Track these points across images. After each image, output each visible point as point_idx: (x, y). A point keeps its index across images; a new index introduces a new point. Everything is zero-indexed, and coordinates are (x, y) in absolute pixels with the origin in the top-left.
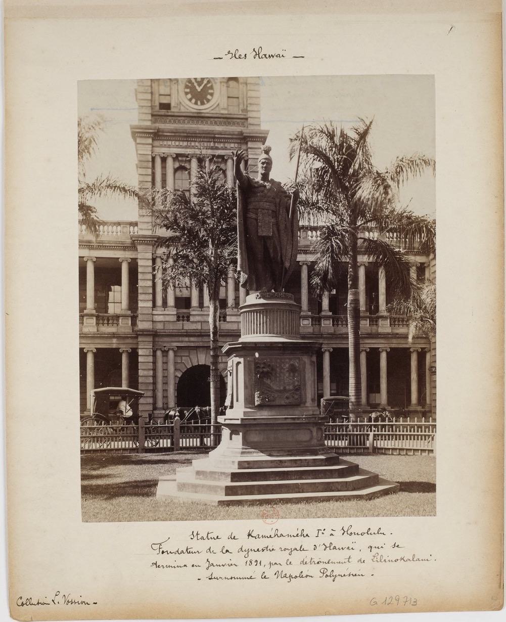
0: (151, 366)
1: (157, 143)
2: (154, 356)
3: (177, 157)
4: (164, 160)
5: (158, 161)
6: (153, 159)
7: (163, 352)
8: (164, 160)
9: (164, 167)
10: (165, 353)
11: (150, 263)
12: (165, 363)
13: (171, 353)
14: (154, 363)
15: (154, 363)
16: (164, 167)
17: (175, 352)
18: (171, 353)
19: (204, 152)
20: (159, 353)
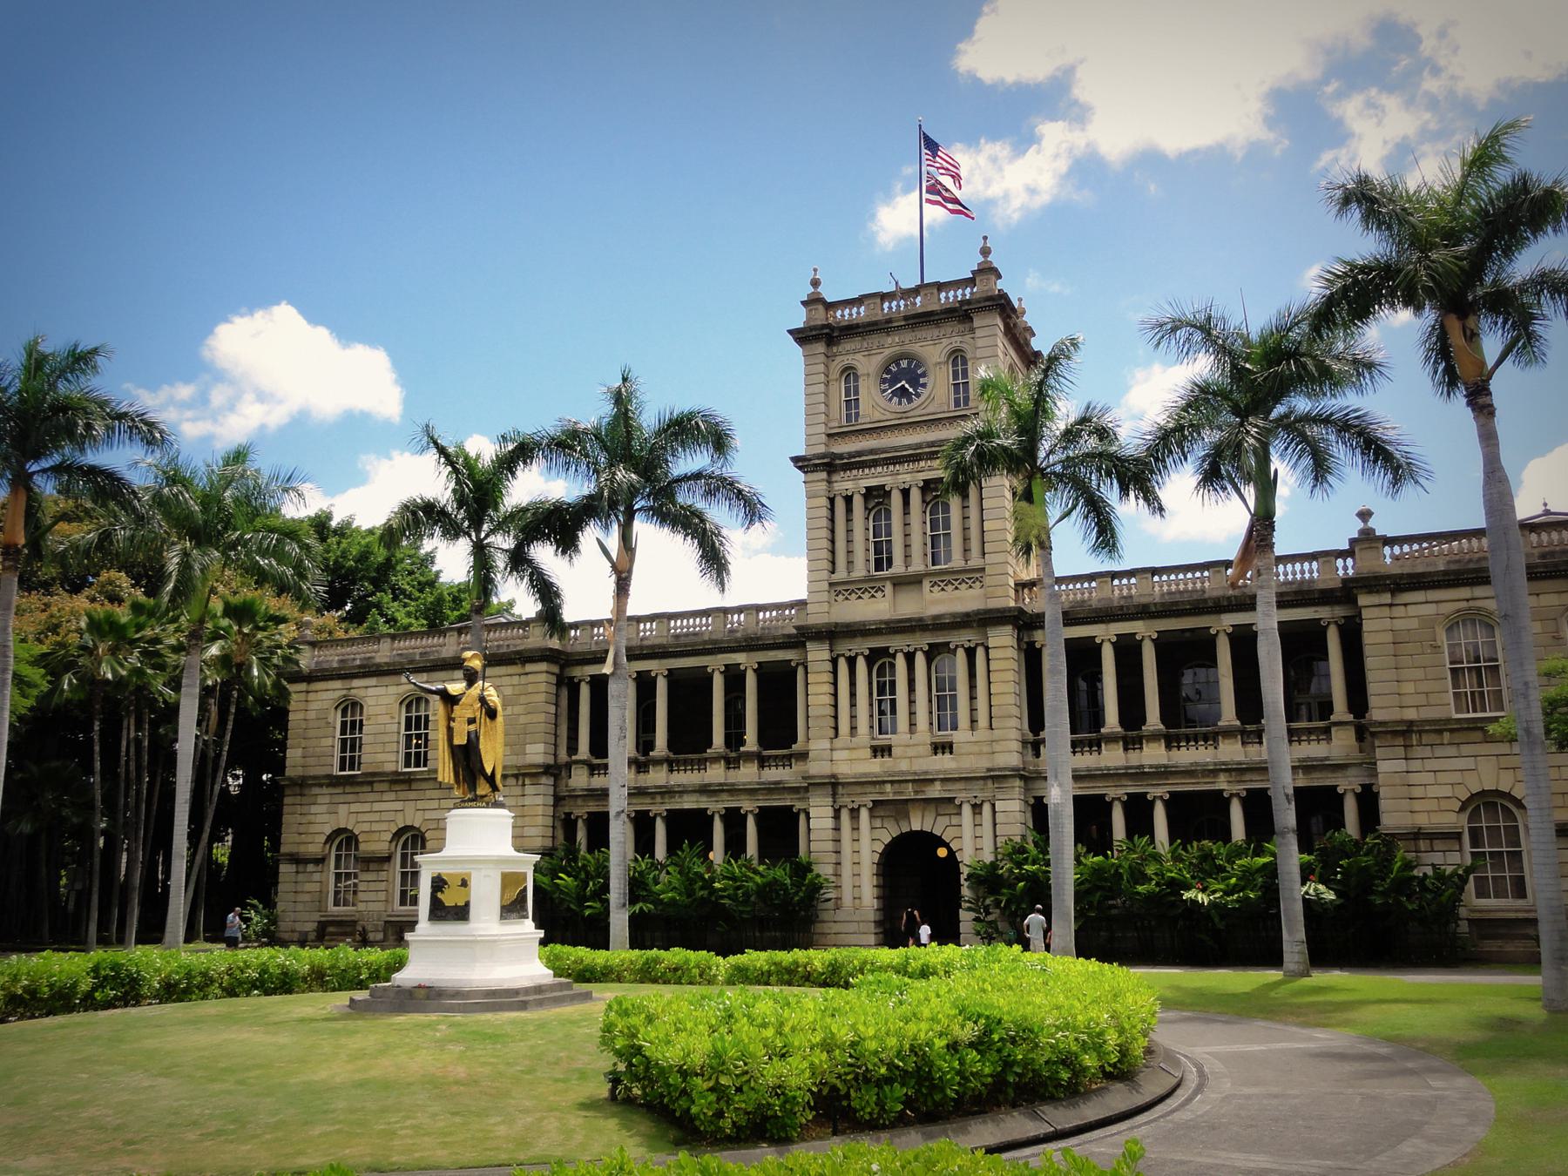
0: (830, 834)
1: (835, 477)
2: (837, 816)
3: (870, 493)
4: (849, 500)
5: (840, 505)
6: (832, 500)
7: (852, 810)
8: (849, 500)
9: (849, 510)
10: (855, 813)
11: (828, 666)
12: (856, 829)
13: (864, 814)
14: (837, 829)
15: (837, 829)
16: (849, 510)
17: (871, 810)
18: (864, 814)
19: (908, 477)
20: (845, 815)
